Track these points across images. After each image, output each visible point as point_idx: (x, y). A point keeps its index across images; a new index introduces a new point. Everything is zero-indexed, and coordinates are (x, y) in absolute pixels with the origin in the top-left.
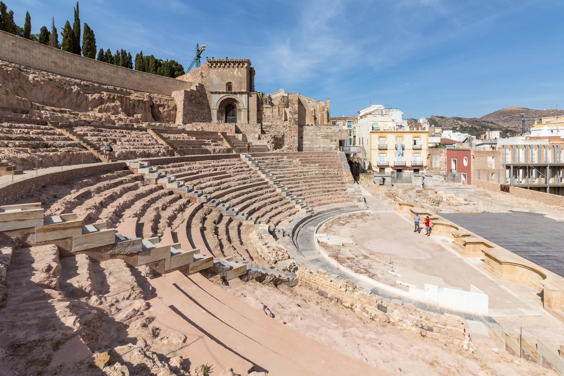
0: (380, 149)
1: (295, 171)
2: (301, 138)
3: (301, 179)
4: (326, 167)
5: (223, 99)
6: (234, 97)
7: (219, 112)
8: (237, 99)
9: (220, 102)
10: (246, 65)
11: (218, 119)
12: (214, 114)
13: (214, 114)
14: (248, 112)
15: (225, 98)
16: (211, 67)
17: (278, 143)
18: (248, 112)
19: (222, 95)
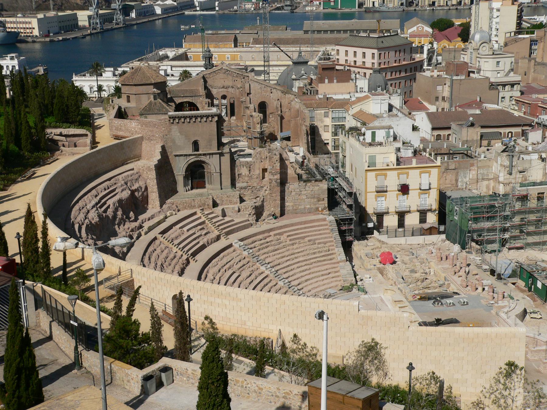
0: (377, 192)
1: (287, 253)
2: (283, 199)
3: (294, 264)
4: (317, 242)
5: (190, 162)
6: (203, 158)
7: (186, 178)
8: (207, 161)
9: (186, 166)
10: (216, 119)
11: (185, 185)
12: (180, 180)
13: (180, 180)
14: (221, 174)
15: (192, 160)
16: (173, 123)
17: (259, 212)
18: (221, 174)
19: (189, 158)
